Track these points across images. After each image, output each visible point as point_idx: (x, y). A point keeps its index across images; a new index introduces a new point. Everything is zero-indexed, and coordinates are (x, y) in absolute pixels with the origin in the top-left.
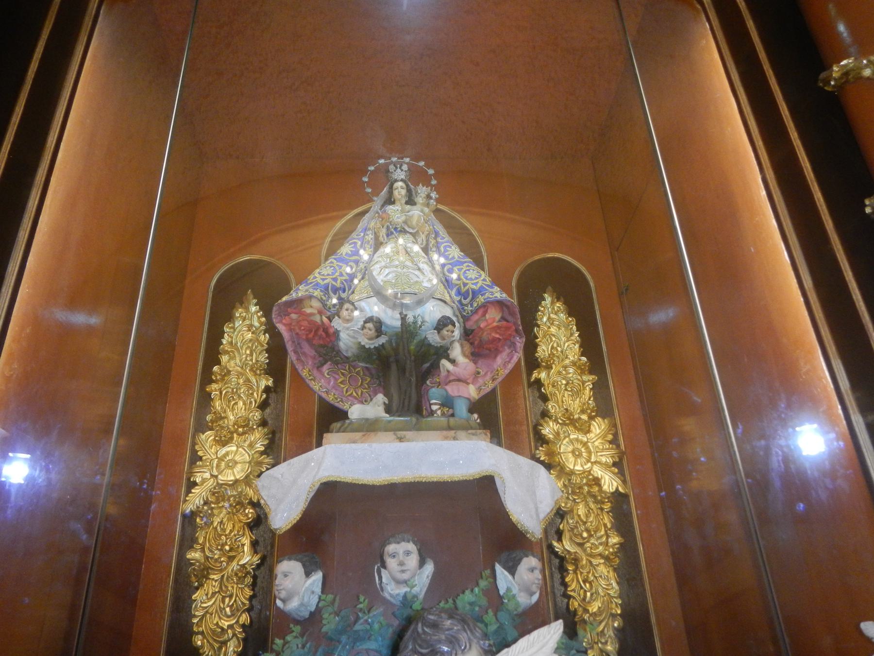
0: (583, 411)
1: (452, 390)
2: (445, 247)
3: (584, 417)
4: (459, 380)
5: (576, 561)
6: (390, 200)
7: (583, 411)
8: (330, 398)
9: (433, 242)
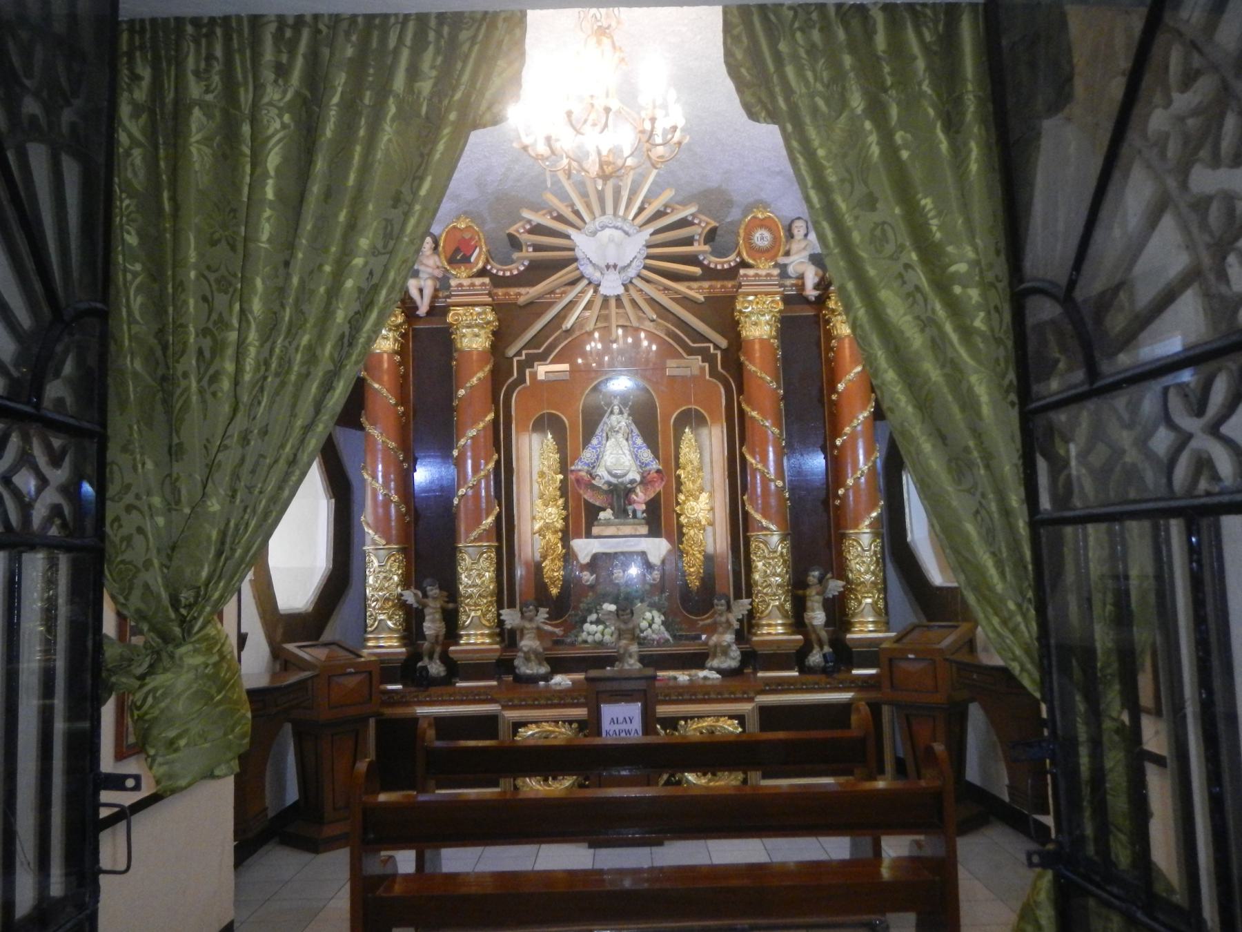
1: (636, 506)
5: (687, 554)
6: (612, 413)
8: (591, 501)
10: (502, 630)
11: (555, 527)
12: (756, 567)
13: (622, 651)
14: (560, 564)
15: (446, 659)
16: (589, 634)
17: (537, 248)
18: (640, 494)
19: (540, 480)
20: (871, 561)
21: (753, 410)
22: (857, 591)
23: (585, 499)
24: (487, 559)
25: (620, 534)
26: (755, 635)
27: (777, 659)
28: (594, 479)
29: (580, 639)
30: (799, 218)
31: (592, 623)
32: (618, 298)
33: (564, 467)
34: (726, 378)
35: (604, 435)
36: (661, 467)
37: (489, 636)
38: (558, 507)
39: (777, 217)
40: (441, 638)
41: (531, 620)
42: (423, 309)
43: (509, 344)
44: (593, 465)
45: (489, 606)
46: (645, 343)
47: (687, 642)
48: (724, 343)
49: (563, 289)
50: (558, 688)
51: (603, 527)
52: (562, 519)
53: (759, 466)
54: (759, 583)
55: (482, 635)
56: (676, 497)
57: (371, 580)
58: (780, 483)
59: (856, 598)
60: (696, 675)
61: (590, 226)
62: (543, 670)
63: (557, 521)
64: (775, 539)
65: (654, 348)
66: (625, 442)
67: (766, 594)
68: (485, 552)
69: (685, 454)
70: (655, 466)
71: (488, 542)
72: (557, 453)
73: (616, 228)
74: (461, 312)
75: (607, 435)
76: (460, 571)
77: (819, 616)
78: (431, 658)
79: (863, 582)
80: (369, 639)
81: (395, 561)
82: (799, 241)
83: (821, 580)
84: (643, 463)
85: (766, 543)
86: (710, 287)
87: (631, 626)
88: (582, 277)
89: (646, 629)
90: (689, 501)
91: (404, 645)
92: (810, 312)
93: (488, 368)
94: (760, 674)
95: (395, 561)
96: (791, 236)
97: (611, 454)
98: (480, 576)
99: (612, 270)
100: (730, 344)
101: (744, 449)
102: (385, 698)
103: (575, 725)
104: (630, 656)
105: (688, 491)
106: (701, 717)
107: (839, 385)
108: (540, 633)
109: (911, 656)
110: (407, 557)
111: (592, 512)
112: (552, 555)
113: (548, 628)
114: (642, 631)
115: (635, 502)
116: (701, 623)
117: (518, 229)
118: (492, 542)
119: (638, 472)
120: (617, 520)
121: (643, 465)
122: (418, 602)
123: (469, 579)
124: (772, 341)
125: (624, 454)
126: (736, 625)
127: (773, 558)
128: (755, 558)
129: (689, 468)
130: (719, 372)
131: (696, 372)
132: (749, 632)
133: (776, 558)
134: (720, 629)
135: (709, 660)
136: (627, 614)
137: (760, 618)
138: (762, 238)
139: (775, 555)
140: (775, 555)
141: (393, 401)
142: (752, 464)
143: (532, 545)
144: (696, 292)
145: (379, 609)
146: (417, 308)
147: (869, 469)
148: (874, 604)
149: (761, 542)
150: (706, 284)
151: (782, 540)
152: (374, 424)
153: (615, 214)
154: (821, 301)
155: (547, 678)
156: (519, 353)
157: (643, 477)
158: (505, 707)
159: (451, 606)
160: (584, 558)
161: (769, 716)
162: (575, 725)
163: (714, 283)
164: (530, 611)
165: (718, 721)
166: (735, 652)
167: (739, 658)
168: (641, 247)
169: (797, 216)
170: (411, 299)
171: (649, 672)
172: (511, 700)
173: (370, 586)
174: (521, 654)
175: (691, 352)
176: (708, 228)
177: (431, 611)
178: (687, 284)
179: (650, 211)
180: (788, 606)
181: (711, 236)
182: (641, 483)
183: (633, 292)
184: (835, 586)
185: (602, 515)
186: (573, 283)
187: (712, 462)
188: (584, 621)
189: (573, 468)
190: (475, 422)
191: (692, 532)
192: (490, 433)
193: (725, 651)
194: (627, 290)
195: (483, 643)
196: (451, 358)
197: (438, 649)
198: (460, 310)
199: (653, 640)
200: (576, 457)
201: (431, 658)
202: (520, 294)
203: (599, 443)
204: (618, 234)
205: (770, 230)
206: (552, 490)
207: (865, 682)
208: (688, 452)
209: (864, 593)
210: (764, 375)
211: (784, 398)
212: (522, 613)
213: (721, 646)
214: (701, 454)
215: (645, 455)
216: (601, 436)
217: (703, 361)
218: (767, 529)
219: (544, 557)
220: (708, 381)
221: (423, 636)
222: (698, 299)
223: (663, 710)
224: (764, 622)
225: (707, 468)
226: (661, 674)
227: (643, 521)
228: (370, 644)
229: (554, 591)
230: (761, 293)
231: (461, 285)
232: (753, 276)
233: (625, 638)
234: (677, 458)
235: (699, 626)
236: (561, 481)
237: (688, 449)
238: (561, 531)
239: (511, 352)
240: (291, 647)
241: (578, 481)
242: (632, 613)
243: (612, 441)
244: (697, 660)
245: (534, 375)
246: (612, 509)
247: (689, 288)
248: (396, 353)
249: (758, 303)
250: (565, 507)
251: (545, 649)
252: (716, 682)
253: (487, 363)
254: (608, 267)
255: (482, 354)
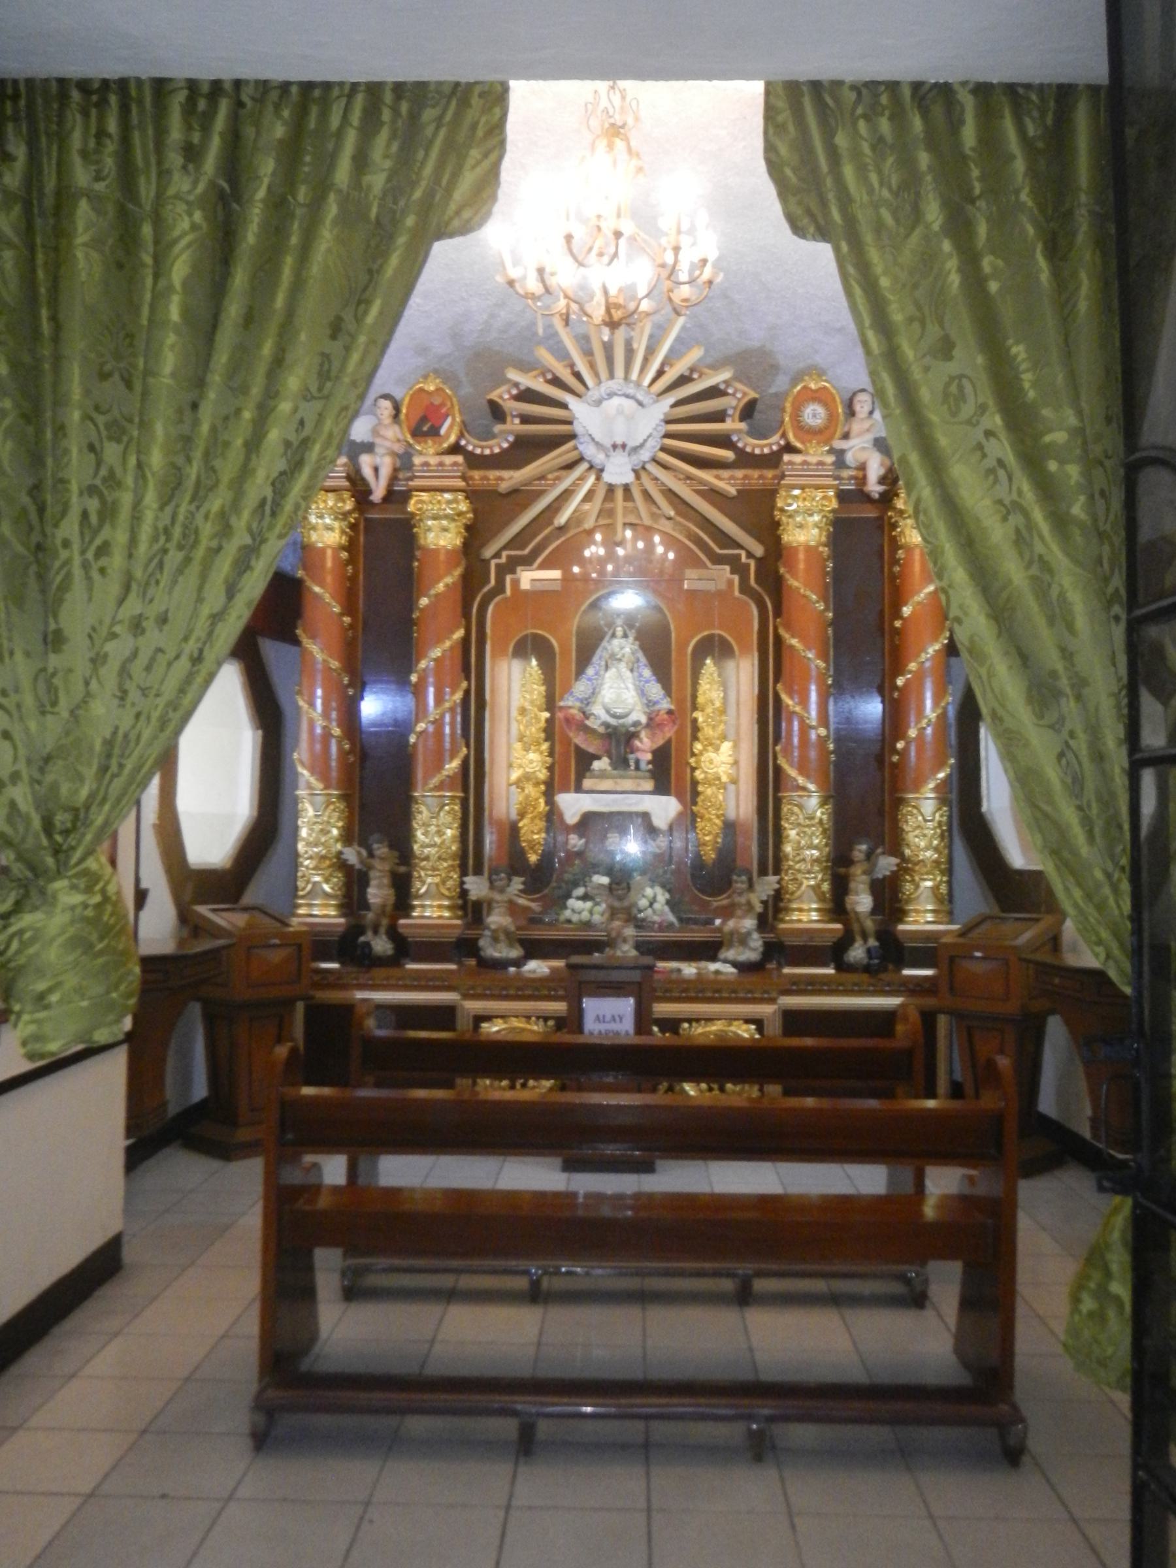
1: (639, 755)
3: (718, 742)
5: (702, 818)
6: (614, 635)
8: (583, 746)
9: (636, 665)
10: (466, 902)
11: (536, 778)
12: (788, 836)
13: (614, 934)
14: (542, 824)
15: (394, 934)
16: (573, 911)
17: (526, 419)
18: (645, 740)
19: (519, 718)
20: (934, 834)
21: (793, 636)
22: (914, 871)
23: (577, 748)
24: (449, 812)
26: (783, 921)
27: (807, 953)
28: (587, 718)
29: (562, 918)
30: (863, 390)
31: (579, 898)
32: (627, 488)
33: (550, 703)
34: (760, 595)
35: (603, 663)
36: (673, 707)
37: (449, 908)
38: (541, 753)
39: (834, 387)
40: (389, 909)
41: (502, 891)
42: (378, 494)
43: (483, 545)
44: (587, 701)
45: (449, 872)
46: (660, 550)
47: (694, 927)
48: (759, 551)
49: (556, 474)
50: (532, 976)
52: (547, 768)
53: (798, 709)
54: (791, 857)
55: (440, 907)
56: (692, 745)
57: (304, 832)
58: (822, 731)
59: (913, 881)
60: (706, 968)
61: (594, 394)
62: (515, 953)
63: (540, 771)
64: (813, 802)
65: (671, 556)
66: (628, 674)
67: (799, 871)
68: (447, 804)
69: (704, 693)
70: (666, 704)
71: (451, 790)
72: (543, 684)
73: (627, 396)
74: (424, 498)
76: (415, 825)
77: (865, 901)
78: (376, 932)
79: (922, 861)
80: (300, 906)
81: (334, 810)
82: (862, 420)
83: (869, 855)
84: (650, 701)
85: (800, 807)
86: (745, 477)
87: (626, 903)
88: (581, 459)
89: (646, 909)
90: (707, 751)
91: (343, 915)
92: (871, 513)
93: (458, 572)
94: (787, 970)
95: (334, 810)
96: (851, 413)
97: (611, 687)
98: (440, 833)
99: (619, 451)
100: (766, 550)
101: (779, 686)
102: (316, 978)
103: (551, 1023)
104: (625, 941)
105: (707, 739)
106: (709, 1020)
107: (905, 609)
108: (513, 909)
109: (978, 954)
110: (350, 806)
111: (585, 761)
112: (532, 812)
113: (522, 901)
114: (640, 911)
115: (638, 750)
116: (715, 904)
117: (502, 395)
118: (458, 792)
119: (645, 713)
120: (615, 772)
121: (650, 703)
122: (362, 862)
123: (427, 837)
124: (821, 549)
125: (627, 688)
126: (759, 908)
127: (809, 826)
128: (786, 825)
129: (709, 710)
130: (753, 589)
131: (722, 586)
132: (775, 918)
133: (813, 826)
134: (739, 912)
135: (723, 950)
136: (623, 889)
137: (790, 901)
138: (814, 416)
139: (813, 822)
140: (813, 822)
141: (337, 610)
142: (788, 706)
143: (508, 799)
144: (726, 483)
145: (314, 869)
146: (370, 492)
147: (938, 717)
148: (935, 889)
149: (796, 805)
150: (739, 473)
151: (823, 804)
152: (313, 637)
153: (626, 378)
154: (887, 499)
155: (518, 963)
156: (497, 555)
157: (650, 719)
158: (466, 996)
159: (402, 869)
160: (571, 818)
161: (794, 1021)
162: (551, 1023)
163: (749, 472)
164: (501, 880)
165: (730, 1025)
166: (756, 941)
167: (761, 949)
168: (657, 422)
169: (861, 387)
170: (363, 479)
171: (647, 960)
172: (473, 988)
173: (304, 839)
174: (487, 933)
175: (718, 560)
176: (746, 400)
177: (378, 874)
178: (715, 472)
179: (671, 375)
180: (826, 887)
181: (748, 411)
182: (648, 726)
183: (645, 479)
184: (886, 864)
185: (596, 765)
186: (570, 466)
187: (738, 705)
188: (568, 896)
189: (562, 704)
190: (439, 641)
191: (709, 791)
192: (458, 653)
193: (743, 940)
194: (638, 477)
195: (440, 917)
196: (412, 558)
197: (385, 922)
198: (425, 496)
199: (654, 923)
200: (567, 689)
201: (376, 932)
202: (501, 479)
203: (597, 674)
204: (629, 404)
205: (825, 405)
206: (535, 731)
207: (918, 985)
208: (709, 689)
209: (922, 874)
210: (808, 593)
211: (834, 623)
212: (491, 882)
213: (738, 932)
214: (725, 692)
215: (654, 691)
216: (599, 665)
217: (732, 572)
218: (804, 789)
219: (522, 815)
220: (738, 599)
221: (366, 906)
222: (728, 492)
223: (663, 1009)
224: (795, 906)
225: (732, 710)
226: (661, 965)
227: (647, 774)
228: (301, 911)
229: (533, 858)
230: (810, 486)
231: (426, 464)
232: (800, 464)
233: (618, 919)
234: (694, 697)
235: (713, 907)
236: (547, 721)
237: (708, 686)
238: (545, 783)
239: (488, 553)
240: (203, 910)
241: (568, 721)
242: (629, 888)
243: (612, 672)
244: (708, 950)
245: (516, 583)
246: (610, 757)
247: (718, 477)
248: (343, 548)
249: (804, 499)
250: (551, 754)
251: (519, 928)
252: (732, 978)
253: (457, 565)
254: (615, 446)
255: (451, 553)
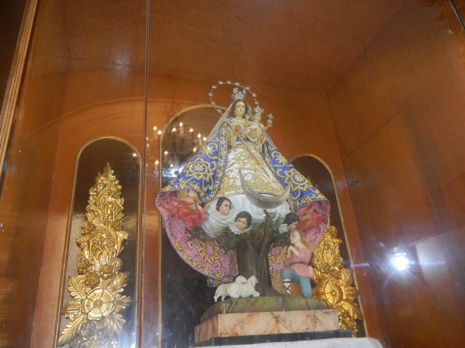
0: (335, 264)
2: (275, 154)
4: (302, 263)
6: (232, 114)
7: (335, 264)
9: (266, 149)
25: (284, 331)
35: (224, 142)
38: (115, 289)
51: (243, 316)
75: (229, 142)
216: (218, 143)
